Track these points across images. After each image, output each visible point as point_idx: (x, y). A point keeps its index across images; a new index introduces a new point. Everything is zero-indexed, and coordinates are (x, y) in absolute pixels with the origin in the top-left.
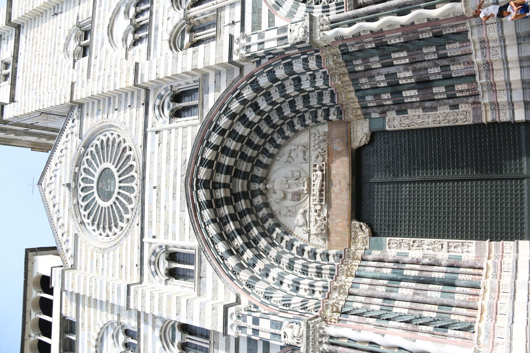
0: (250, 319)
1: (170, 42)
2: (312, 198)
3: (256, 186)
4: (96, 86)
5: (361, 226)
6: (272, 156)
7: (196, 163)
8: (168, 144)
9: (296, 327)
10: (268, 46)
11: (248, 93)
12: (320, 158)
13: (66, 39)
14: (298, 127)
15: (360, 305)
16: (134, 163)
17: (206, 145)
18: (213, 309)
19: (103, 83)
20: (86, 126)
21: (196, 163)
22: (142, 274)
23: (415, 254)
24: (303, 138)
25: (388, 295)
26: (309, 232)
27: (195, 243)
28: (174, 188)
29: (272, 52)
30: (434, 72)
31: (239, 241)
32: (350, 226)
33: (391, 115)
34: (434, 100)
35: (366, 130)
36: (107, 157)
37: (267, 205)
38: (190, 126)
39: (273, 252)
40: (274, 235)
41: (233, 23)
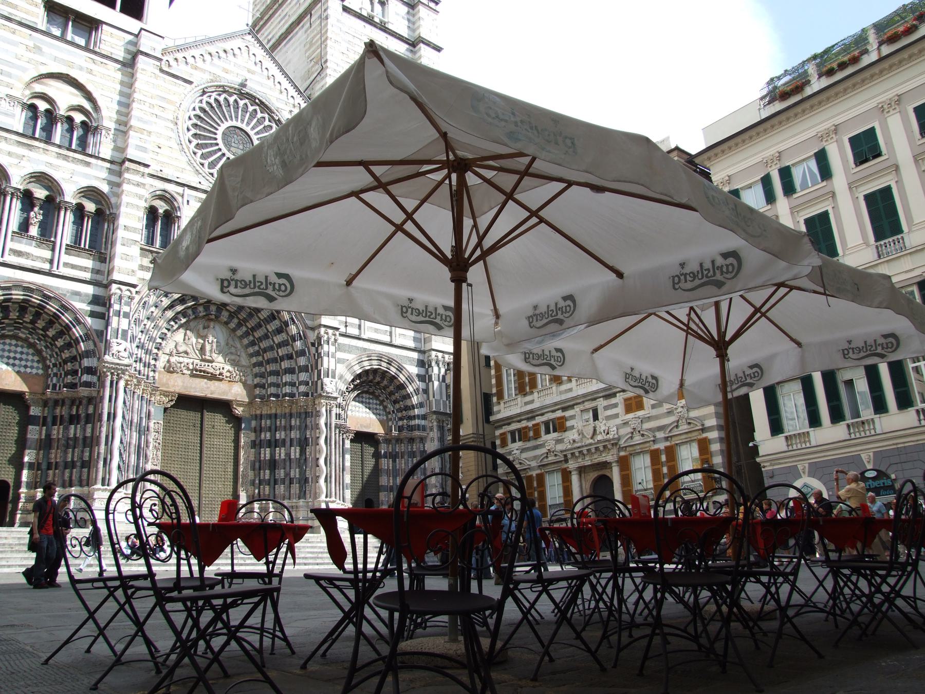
0: (126, 309)
2: (196, 362)
6: (234, 330)
9: (126, 354)
12: (228, 374)
14: (254, 360)
18: (133, 271)
26: (171, 355)
29: (320, 360)
30: (281, 473)
33: (253, 436)
34: (260, 469)
39: (162, 323)
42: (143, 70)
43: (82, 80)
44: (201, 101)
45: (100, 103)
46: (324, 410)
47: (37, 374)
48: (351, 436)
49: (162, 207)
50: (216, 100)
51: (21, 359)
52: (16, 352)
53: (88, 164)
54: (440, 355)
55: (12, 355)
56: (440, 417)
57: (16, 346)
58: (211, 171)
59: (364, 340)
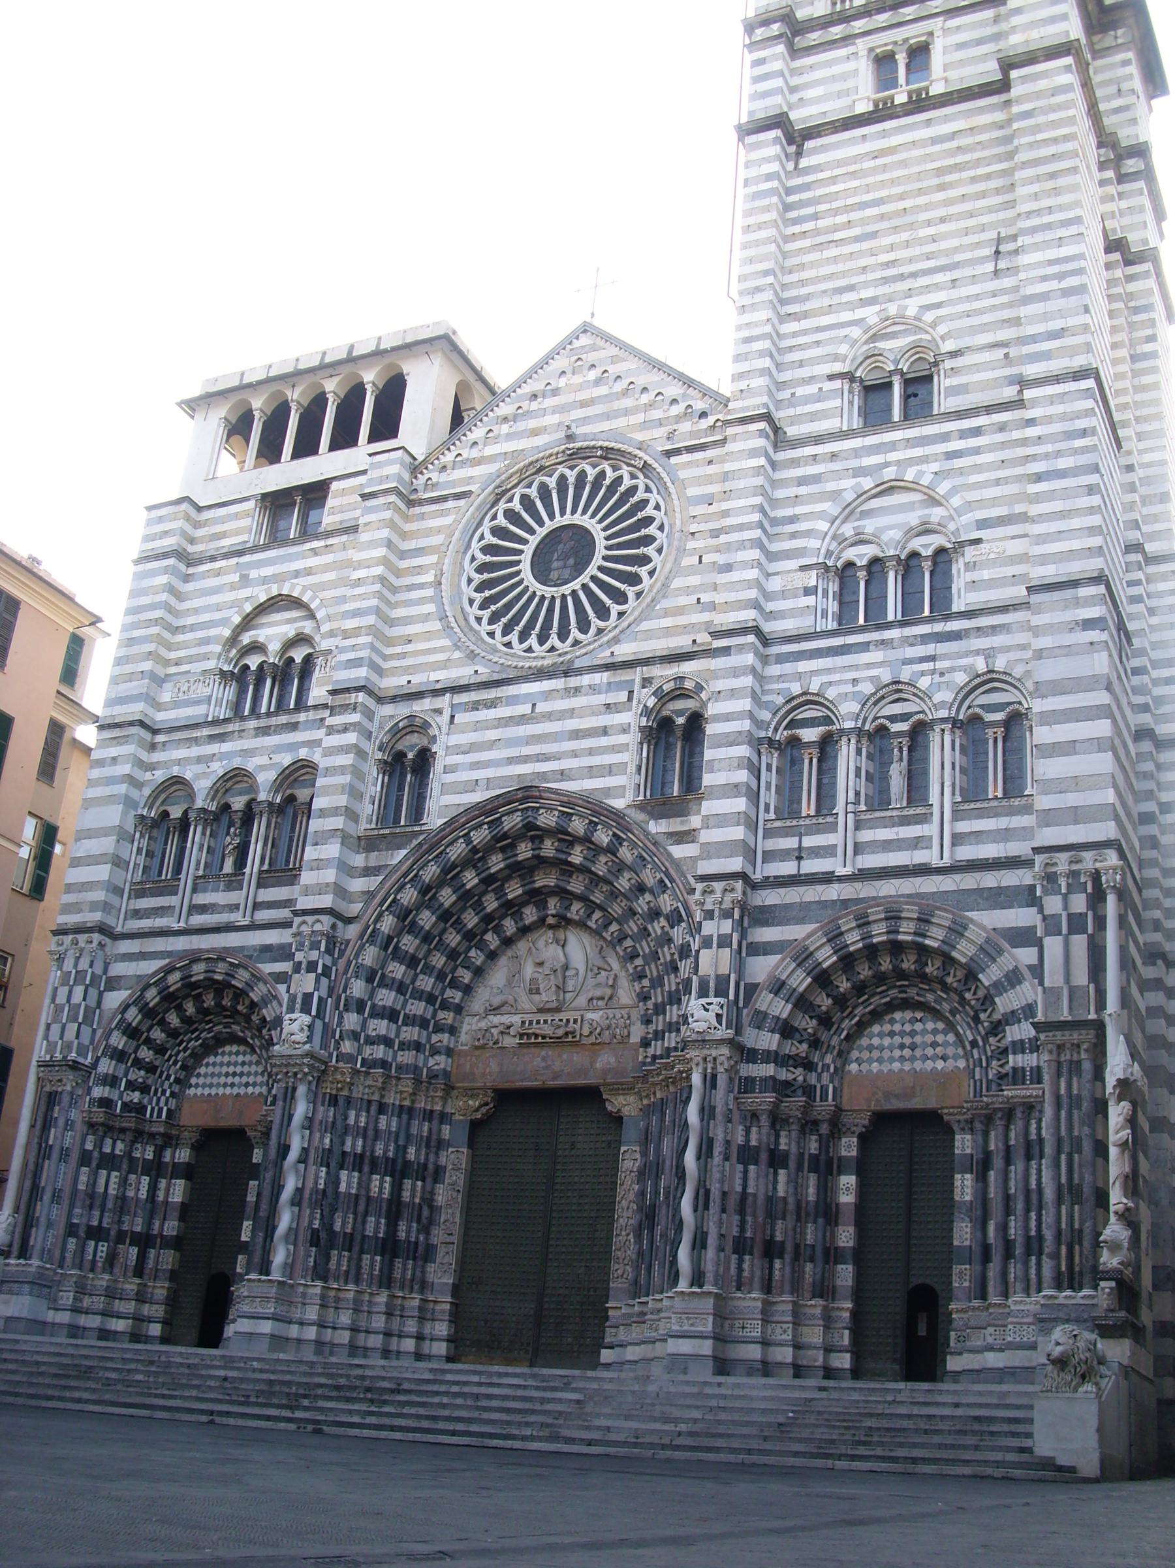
0: (314, 955)
1: (804, 694)
3: (553, 906)
4: (741, 503)
5: (487, 1104)
7: (563, 804)
8: (605, 731)
9: (301, 1037)
10: (706, 956)
11: (666, 902)
13: (915, 318)
15: (351, 1121)
16: (593, 630)
17: (591, 822)
19: (741, 527)
20: (690, 464)
21: (563, 804)
22: (394, 699)
23: (442, 1195)
24: (626, 994)
25: (367, 1161)
27: (434, 820)
28: (525, 759)
31: (447, 897)
32: (484, 1088)
35: (626, 1111)
36: (619, 546)
37: (524, 931)
38: (622, 788)
39: (438, 960)
40: (473, 953)
41: (799, 858)
42: (366, 524)
43: (295, 594)
44: (494, 517)
45: (319, 615)
46: (696, 1079)
47: (260, 1094)
48: (863, 1121)
49: (410, 745)
50: (525, 499)
51: (242, 1074)
52: (236, 1064)
53: (294, 727)
54: (1063, 857)
55: (231, 1069)
56: (1059, 1036)
57: (237, 1053)
58: (506, 639)
59: (841, 879)
